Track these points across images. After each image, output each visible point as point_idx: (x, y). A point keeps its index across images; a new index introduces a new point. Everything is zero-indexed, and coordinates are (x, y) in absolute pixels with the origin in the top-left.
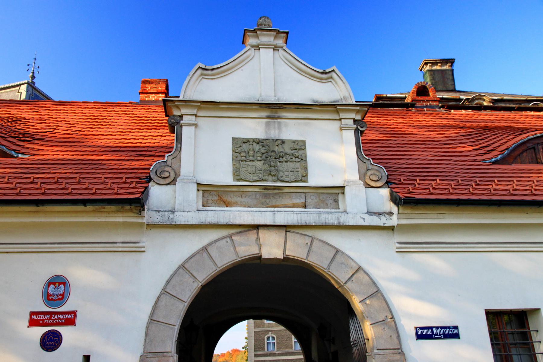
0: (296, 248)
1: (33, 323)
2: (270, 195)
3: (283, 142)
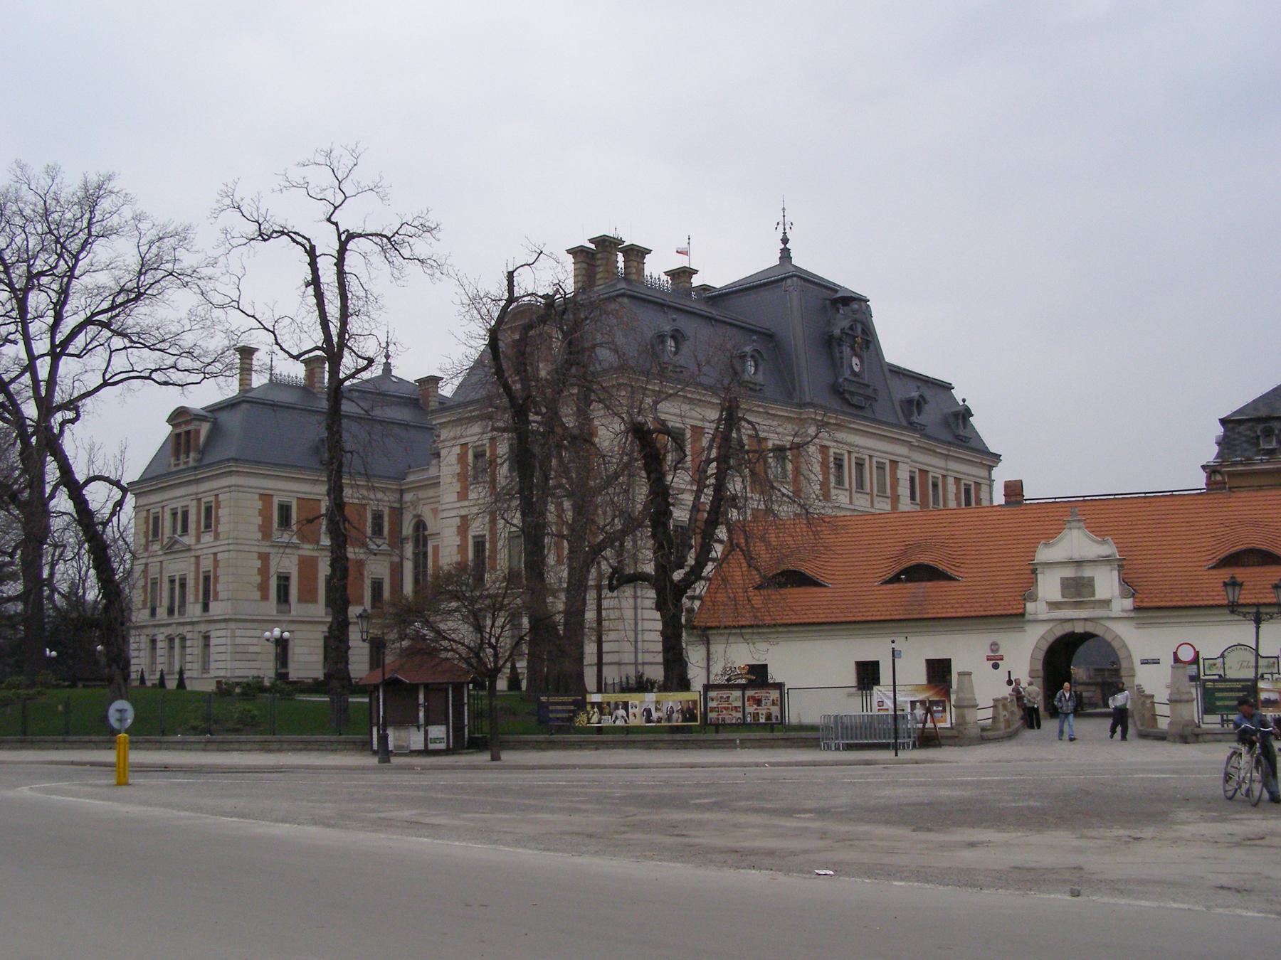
0: (1090, 628)
1: (989, 659)
2: (1077, 605)
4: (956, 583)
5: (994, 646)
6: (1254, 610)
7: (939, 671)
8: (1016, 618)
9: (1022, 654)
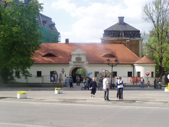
2: (78, 62)
3: (79, 57)
4: (56, 57)
5: (63, 69)
6: (112, 65)
7: (52, 73)
8: (67, 64)
9: (68, 70)
